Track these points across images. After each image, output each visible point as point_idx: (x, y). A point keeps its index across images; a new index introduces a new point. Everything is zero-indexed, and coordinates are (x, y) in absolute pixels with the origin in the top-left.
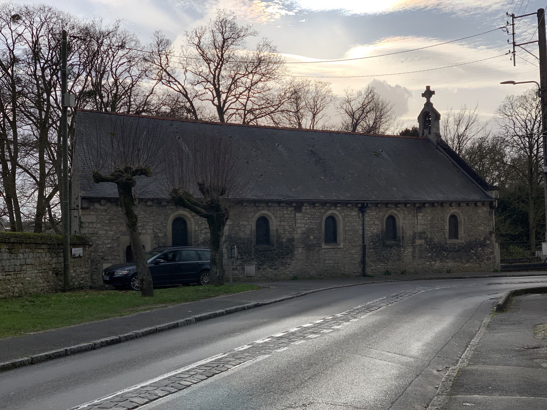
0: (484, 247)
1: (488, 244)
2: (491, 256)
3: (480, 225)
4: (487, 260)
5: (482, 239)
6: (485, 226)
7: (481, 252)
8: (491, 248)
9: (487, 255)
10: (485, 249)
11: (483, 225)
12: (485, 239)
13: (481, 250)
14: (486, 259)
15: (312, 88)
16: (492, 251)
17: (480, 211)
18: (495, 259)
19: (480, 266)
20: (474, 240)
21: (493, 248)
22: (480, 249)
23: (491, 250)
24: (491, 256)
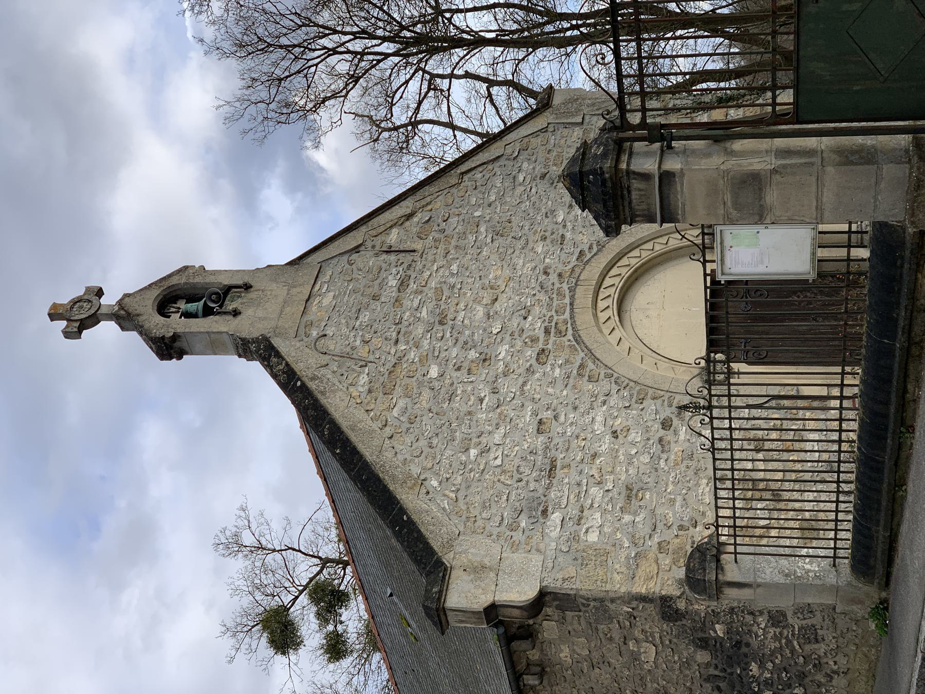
0: (744, 650)
1: (728, 632)
2: (796, 623)
3: (635, 657)
4: (817, 641)
5: (703, 657)
6: (637, 633)
7: (770, 665)
8: (749, 618)
9: (789, 642)
10: (754, 643)
11: (631, 645)
12: (704, 643)
13: (762, 666)
14: (808, 647)
15: (247, 601)
16: (766, 616)
17: (565, 654)
18: (815, 607)
19: (845, 673)
20: (708, 686)
21: (752, 613)
22: (754, 668)
23: (762, 621)
24: (796, 623)
